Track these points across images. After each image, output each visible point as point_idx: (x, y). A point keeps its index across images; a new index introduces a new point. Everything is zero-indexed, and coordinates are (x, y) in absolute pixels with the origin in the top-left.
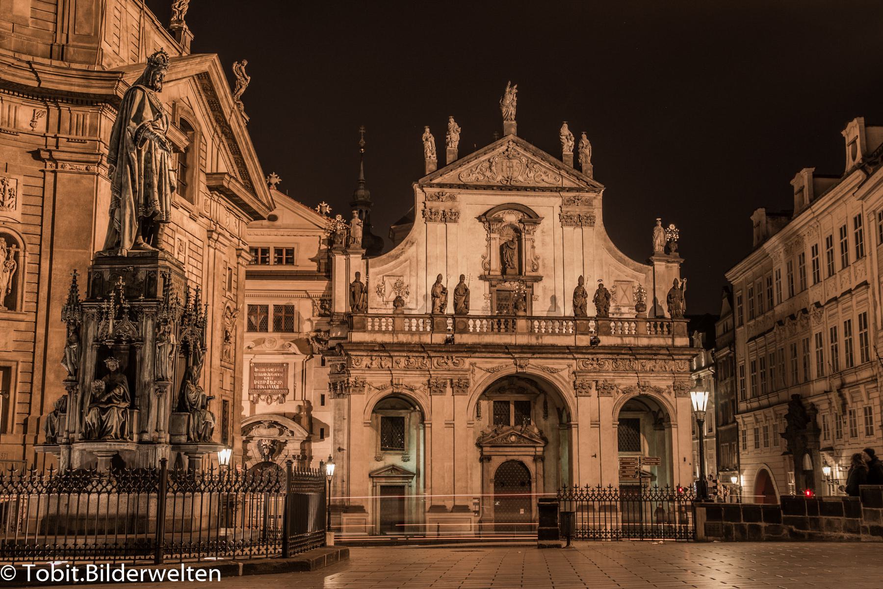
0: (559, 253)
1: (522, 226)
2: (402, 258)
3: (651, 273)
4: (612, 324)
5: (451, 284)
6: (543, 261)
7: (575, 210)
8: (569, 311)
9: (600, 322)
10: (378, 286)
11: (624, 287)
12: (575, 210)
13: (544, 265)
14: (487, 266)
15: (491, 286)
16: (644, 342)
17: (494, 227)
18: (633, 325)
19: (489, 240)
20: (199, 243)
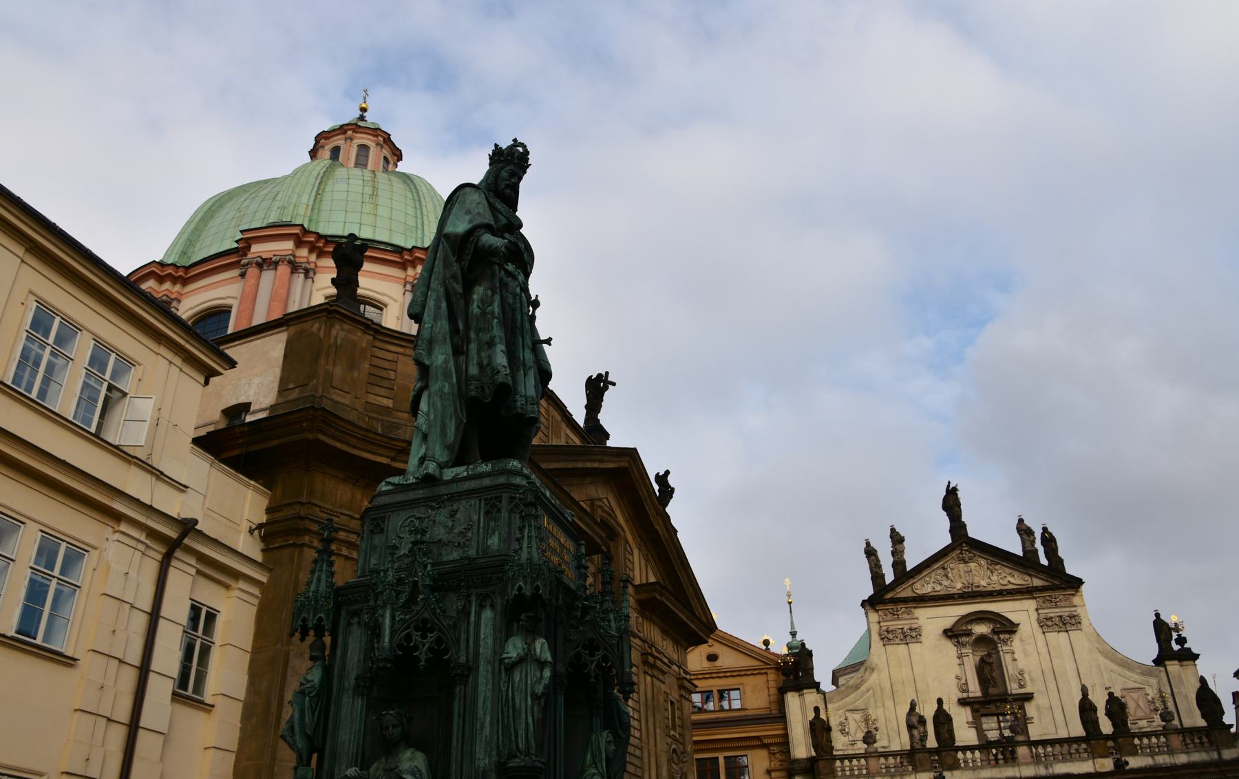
0: (1046, 664)
1: (995, 638)
2: (863, 688)
3: (1163, 675)
4: (1136, 741)
5: (928, 711)
6: (1029, 673)
7: (1053, 612)
8: (1078, 730)
9: (1120, 740)
10: (841, 723)
11: (1135, 695)
12: (1053, 612)
13: (1032, 680)
14: (964, 688)
15: (974, 711)
16: (1182, 759)
17: (964, 639)
18: (1163, 739)
19: (960, 657)
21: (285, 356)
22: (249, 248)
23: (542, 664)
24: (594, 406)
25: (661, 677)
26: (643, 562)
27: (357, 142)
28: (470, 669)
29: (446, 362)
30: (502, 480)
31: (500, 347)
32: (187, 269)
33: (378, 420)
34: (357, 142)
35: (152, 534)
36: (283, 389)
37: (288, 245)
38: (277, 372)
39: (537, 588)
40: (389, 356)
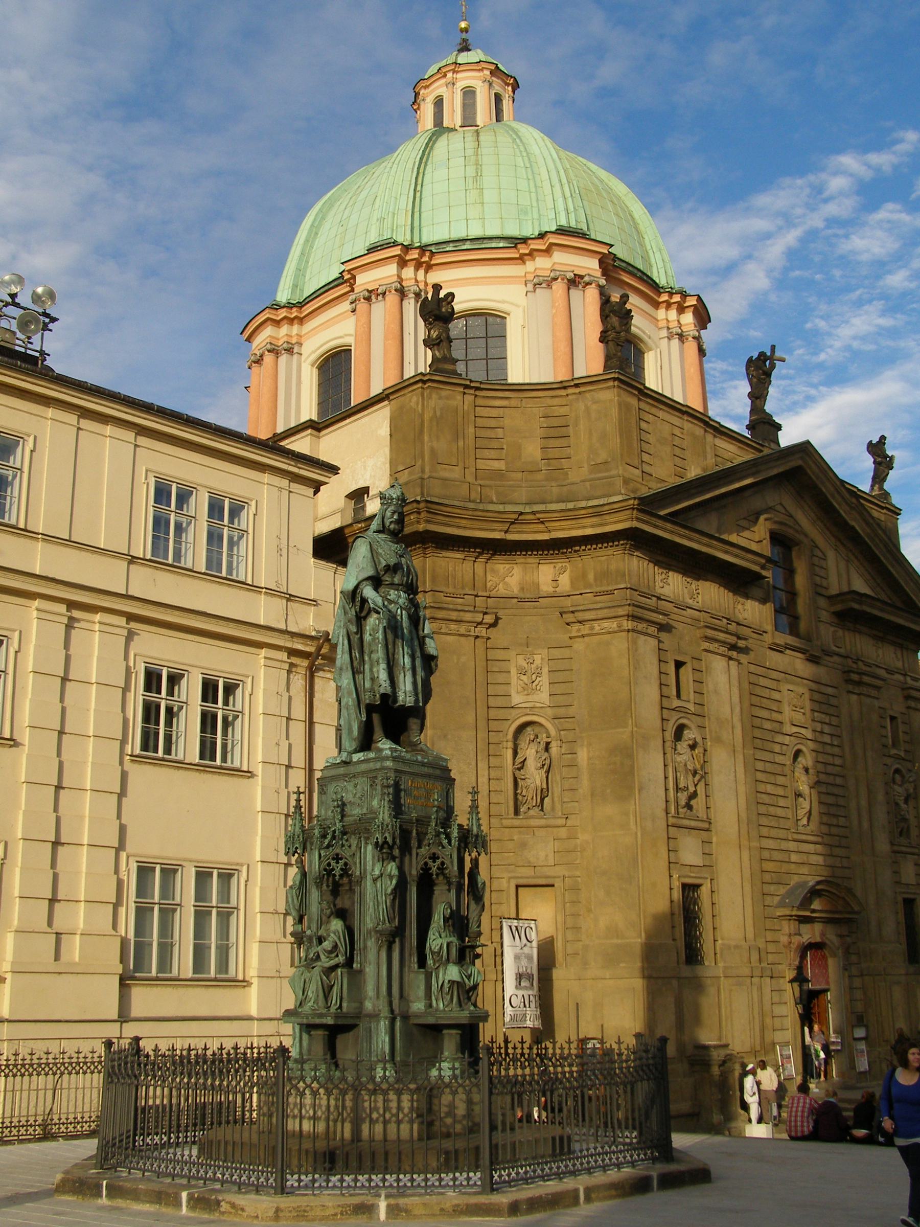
20: (830, 691)
21: (391, 435)
22: (354, 277)
23: (391, 877)
24: (758, 396)
25: (873, 693)
26: (842, 565)
27: (460, 85)
28: (362, 877)
29: (349, 684)
30: (378, 765)
31: (383, 666)
32: (301, 305)
33: (490, 486)
34: (460, 85)
35: (292, 652)
37: (391, 270)
38: (387, 450)
39: (386, 838)
40: (494, 413)
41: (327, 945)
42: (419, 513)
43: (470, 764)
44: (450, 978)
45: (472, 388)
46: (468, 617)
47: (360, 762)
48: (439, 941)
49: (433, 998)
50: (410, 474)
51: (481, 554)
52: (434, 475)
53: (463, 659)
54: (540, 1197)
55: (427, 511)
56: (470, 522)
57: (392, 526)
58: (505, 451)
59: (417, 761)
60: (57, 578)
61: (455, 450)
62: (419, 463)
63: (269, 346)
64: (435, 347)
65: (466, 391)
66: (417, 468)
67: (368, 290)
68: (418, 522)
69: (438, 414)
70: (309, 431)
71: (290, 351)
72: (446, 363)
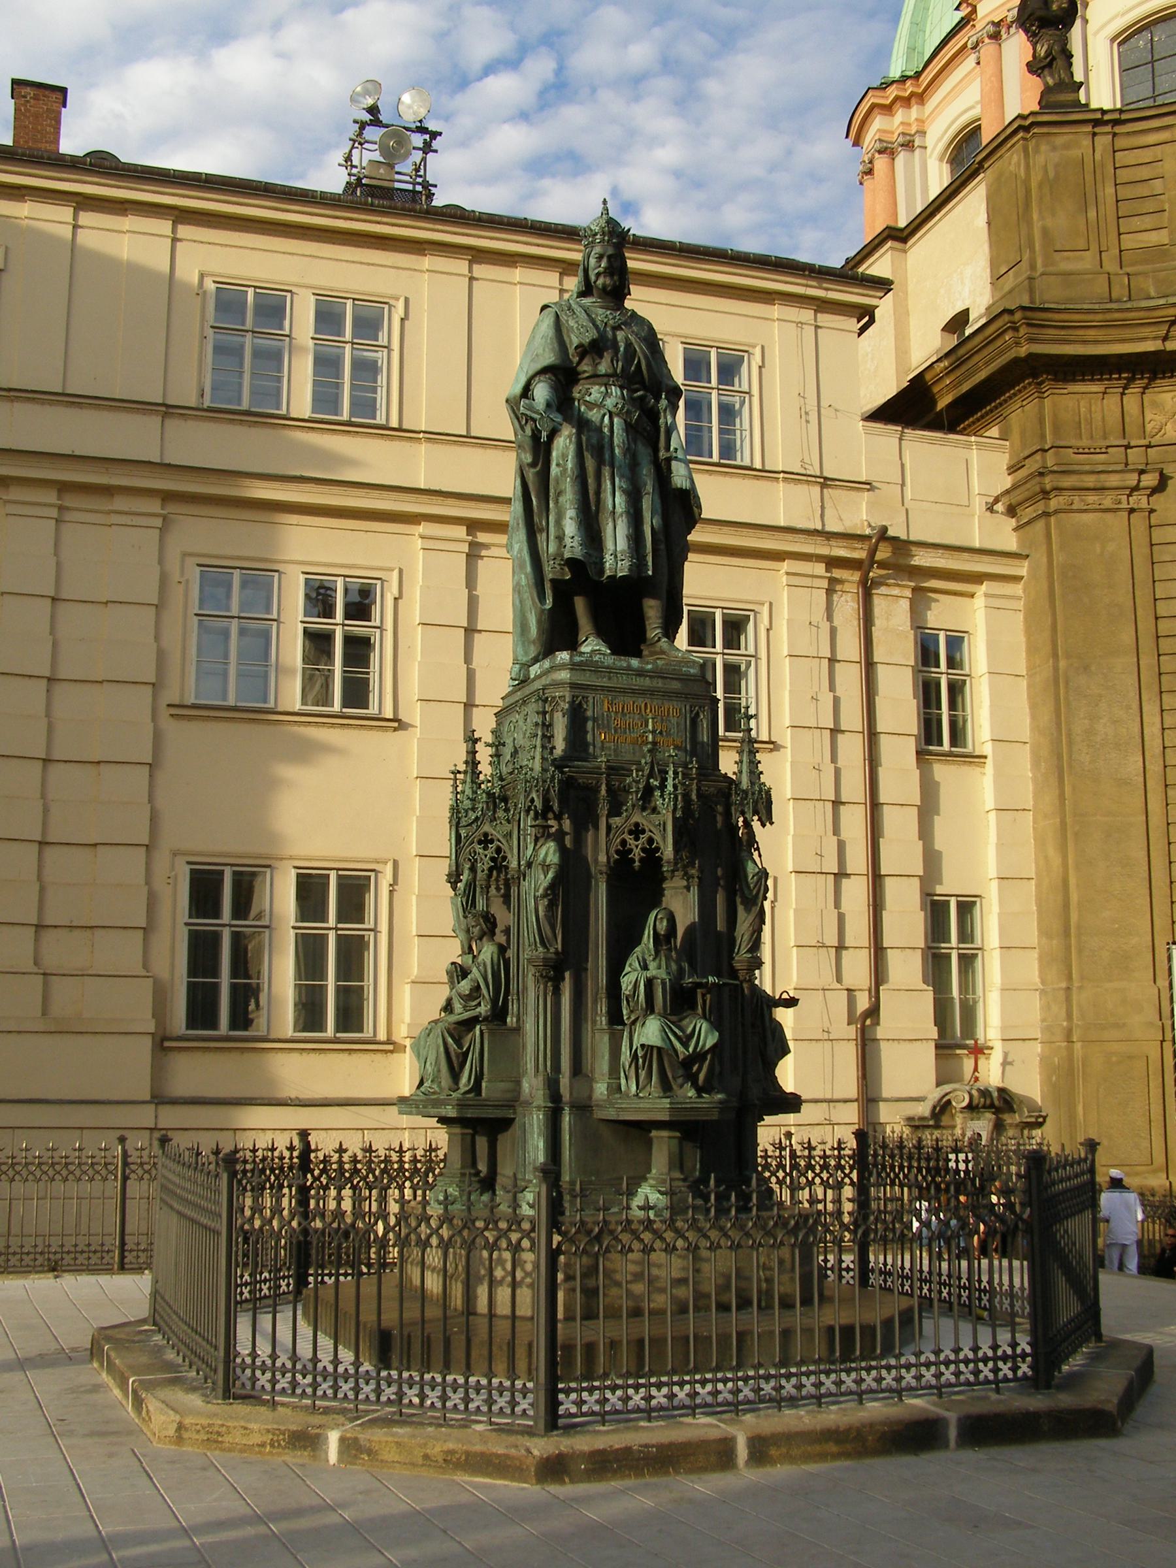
21: (989, 223)
23: (546, 867)
35: (832, 563)
36: (996, 279)
38: (986, 248)
39: (532, 801)
41: (465, 986)
42: (1016, 329)
43: (1128, 707)
44: (643, 1041)
45: (1107, 123)
46: (1113, 480)
47: (538, 677)
48: (632, 977)
49: (622, 1074)
50: (1016, 276)
51: (1131, 380)
52: (1051, 269)
53: (1111, 547)
54: (628, 1450)
55: (1029, 325)
56: (1102, 332)
57: (600, 281)
58: (1166, 213)
59: (629, 668)
60: (444, 489)
61: (1083, 227)
62: (1026, 257)
63: (878, 146)
64: (1046, 72)
65: (1097, 130)
66: (1024, 264)
67: (993, 23)
68: (1017, 344)
69: (1051, 174)
70: (889, 244)
71: (909, 145)
72: (1061, 92)
